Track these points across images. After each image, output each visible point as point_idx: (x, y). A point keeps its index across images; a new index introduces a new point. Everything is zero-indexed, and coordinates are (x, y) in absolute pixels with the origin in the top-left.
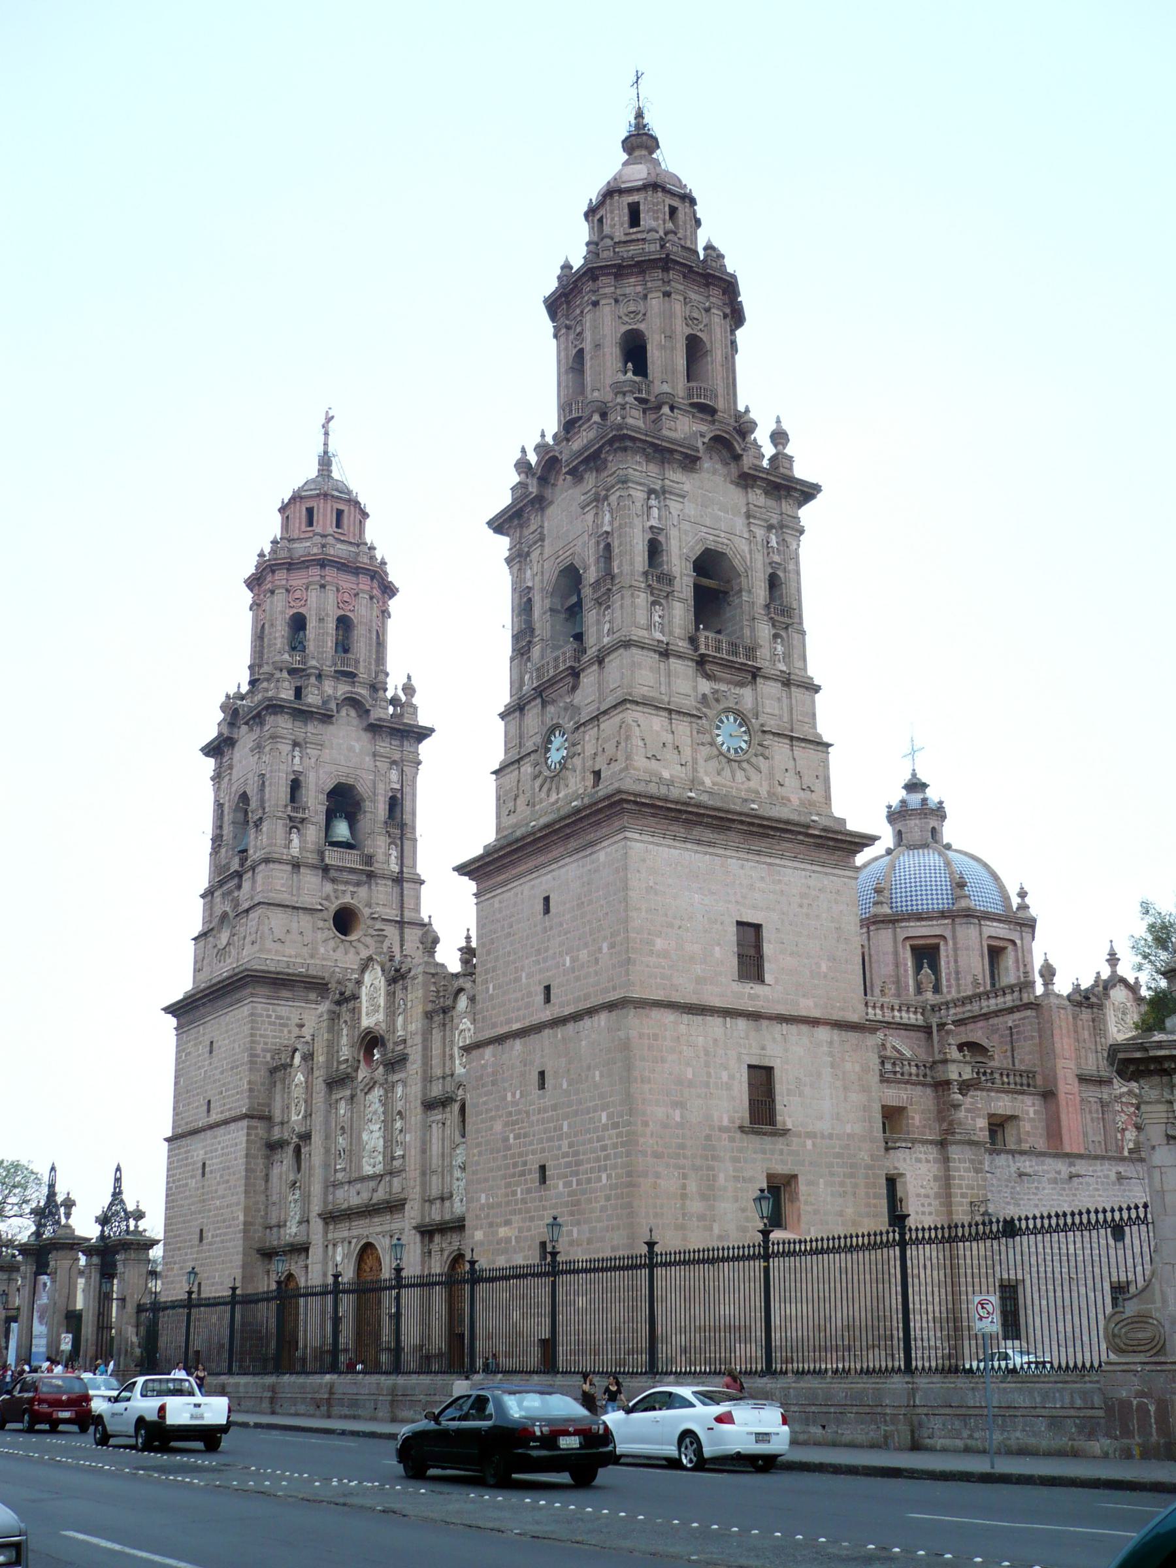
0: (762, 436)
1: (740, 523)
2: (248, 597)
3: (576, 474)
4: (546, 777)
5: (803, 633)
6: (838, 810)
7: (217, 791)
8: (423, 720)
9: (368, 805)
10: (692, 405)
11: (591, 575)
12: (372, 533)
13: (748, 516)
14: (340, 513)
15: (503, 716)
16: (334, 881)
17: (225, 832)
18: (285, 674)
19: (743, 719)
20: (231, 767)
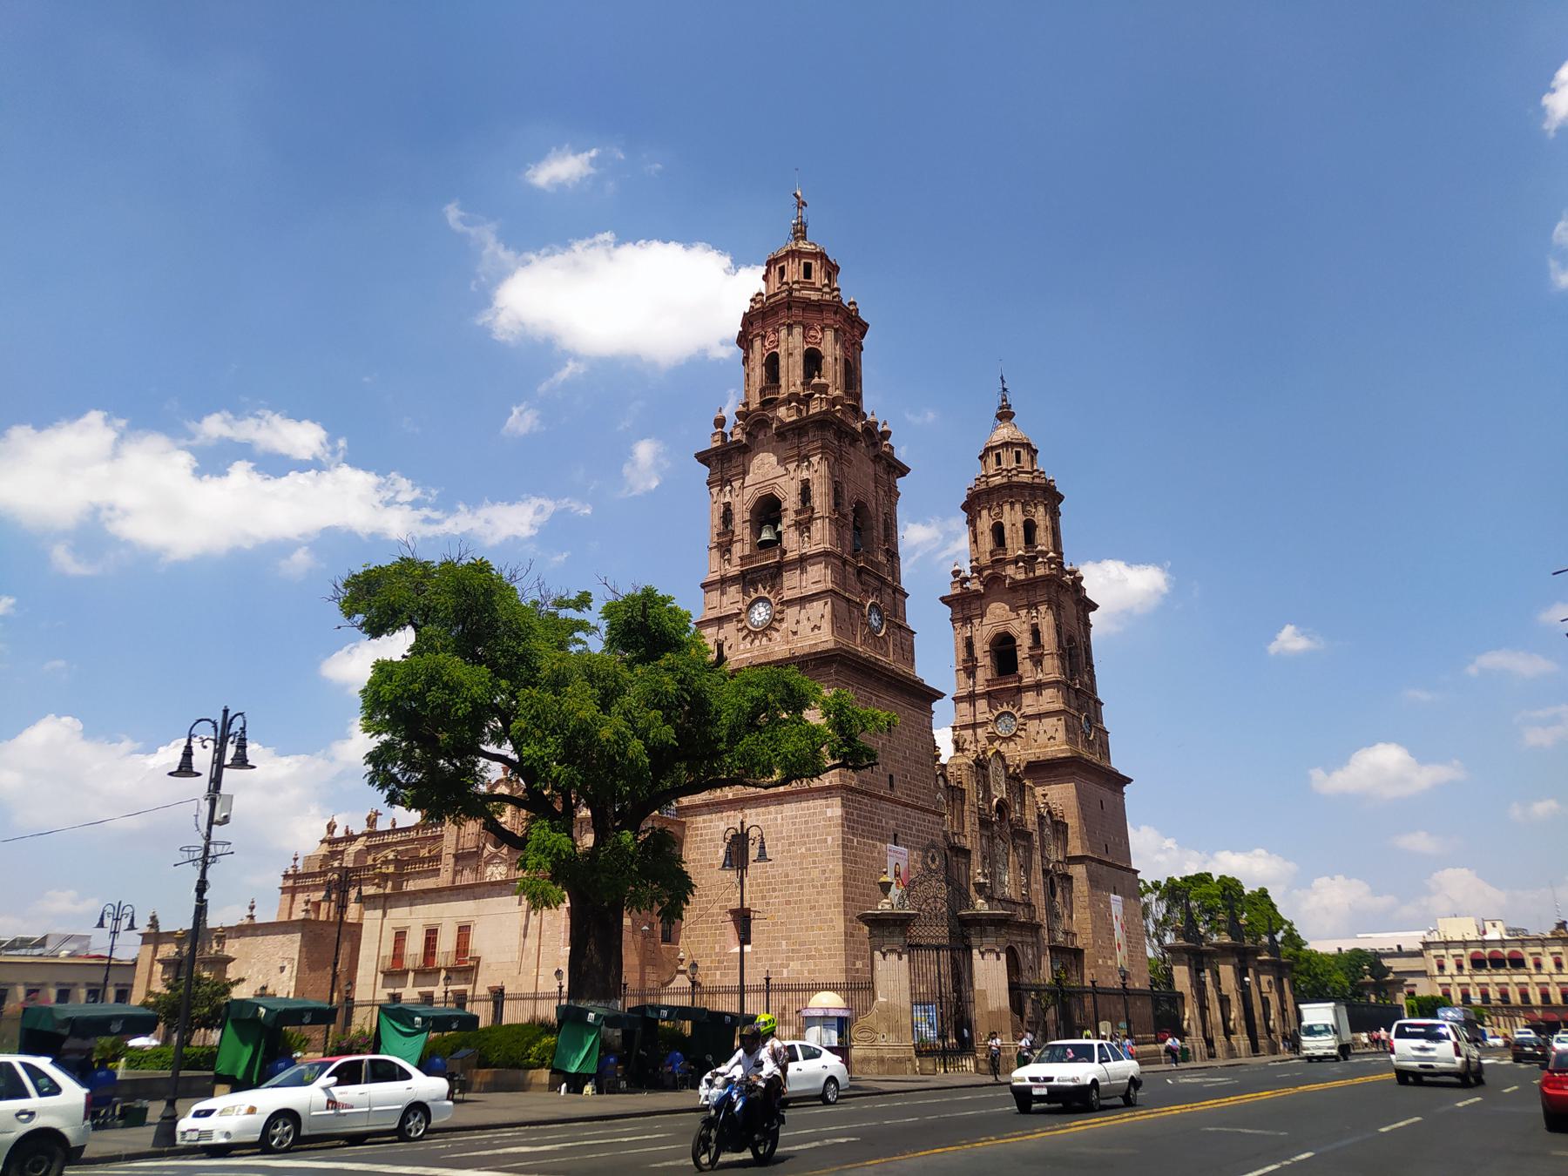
1: (872, 485)
4: (750, 631)
11: (791, 502)
13: (876, 483)
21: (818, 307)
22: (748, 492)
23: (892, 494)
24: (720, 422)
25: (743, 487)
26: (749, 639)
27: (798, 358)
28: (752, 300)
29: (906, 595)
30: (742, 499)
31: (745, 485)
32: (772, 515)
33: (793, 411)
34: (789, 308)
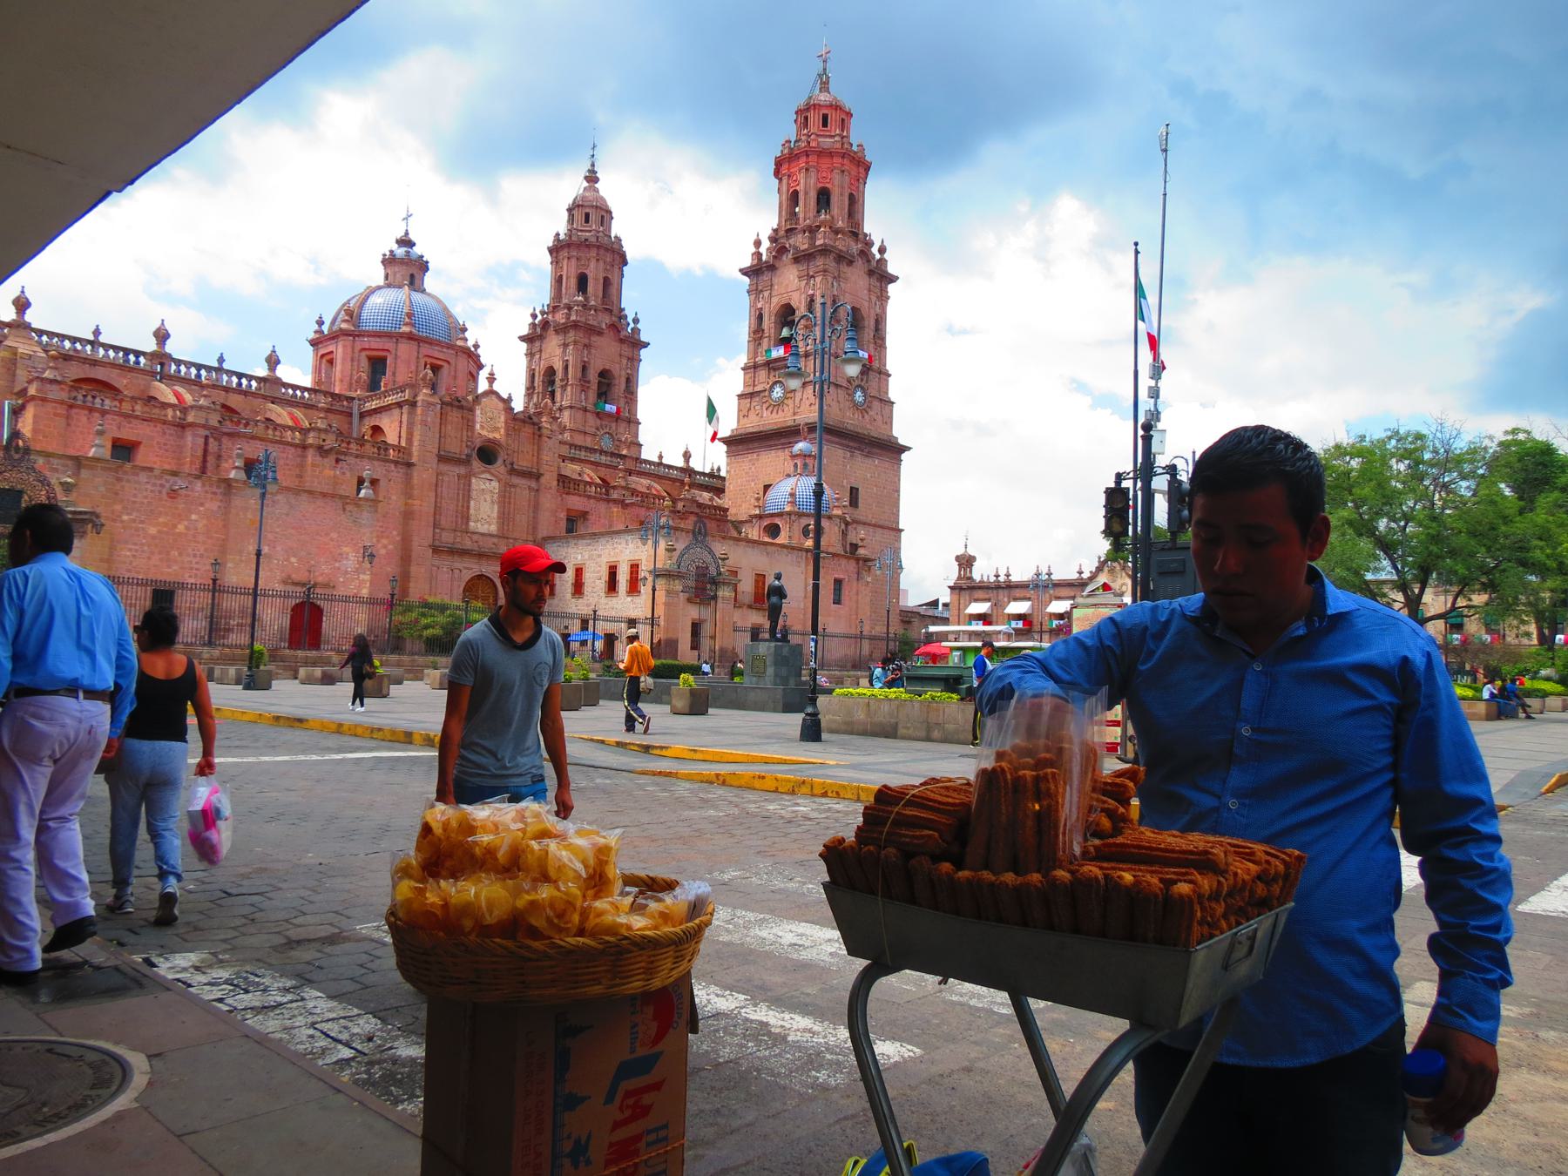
0: (875, 250)
2: (548, 258)
3: (796, 260)
5: (885, 348)
6: (895, 433)
7: (530, 362)
8: (643, 338)
9: (617, 382)
10: (851, 232)
11: (801, 310)
12: (616, 229)
13: (870, 290)
14: (603, 217)
15: (743, 369)
16: (600, 419)
17: (536, 385)
18: (580, 308)
19: (864, 390)
20: (541, 351)
21: (830, 154)
22: (775, 300)
23: (883, 298)
24: (758, 243)
25: (771, 296)
26: (771, 409)
27: (813, 195)
28: (783, 145)
29: (889, 375)
30: (771, 306)
31: (774, 293)
32: (790, 318)
33: (806, 241)
34: (807, 156)
